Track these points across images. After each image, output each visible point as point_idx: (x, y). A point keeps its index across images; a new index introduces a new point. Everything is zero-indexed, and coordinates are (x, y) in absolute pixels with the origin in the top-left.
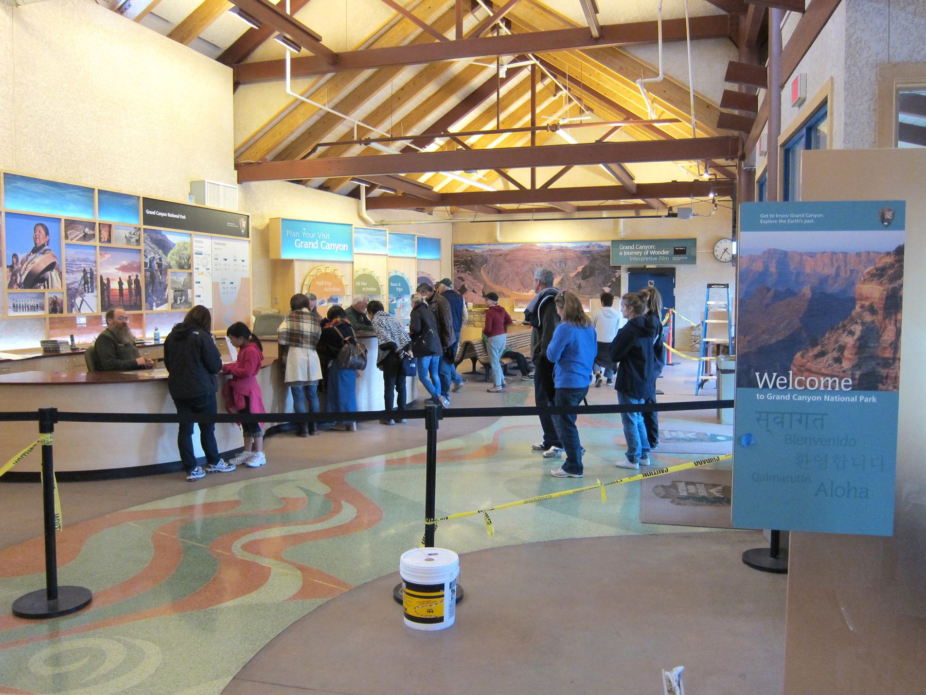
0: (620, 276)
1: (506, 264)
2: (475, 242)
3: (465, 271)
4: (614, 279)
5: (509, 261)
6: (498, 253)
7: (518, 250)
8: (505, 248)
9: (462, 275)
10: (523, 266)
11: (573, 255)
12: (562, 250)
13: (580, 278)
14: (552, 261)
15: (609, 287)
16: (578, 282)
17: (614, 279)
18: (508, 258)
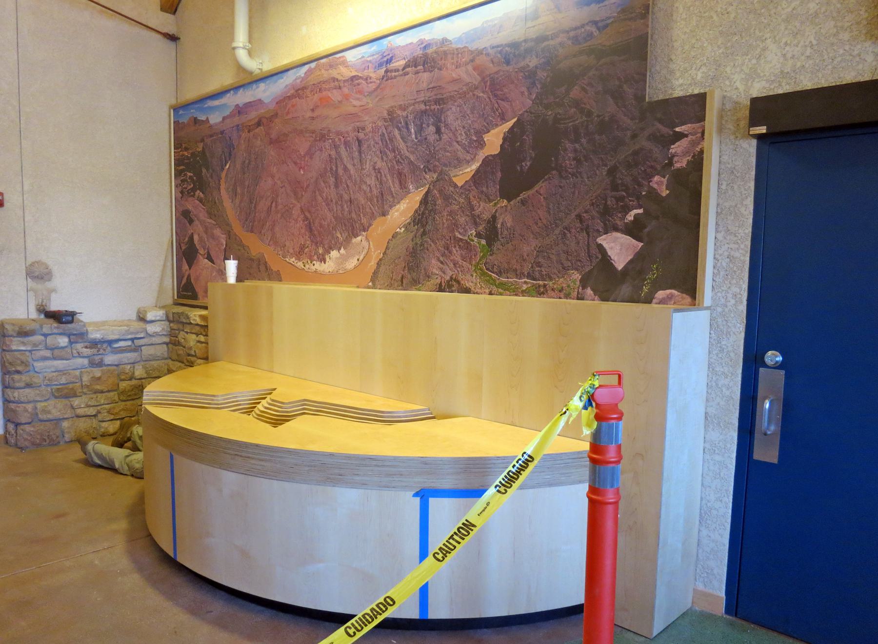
0: (698, 163)
1: (272, 153)
2: (213, 86)
3: (194, 190)
4: (660, 184)
5: (276, 142)
6: (253, 115)
7: (298, 92)
8: (267, 93)
9: (191, 204)
10: (310, 154)
11: (468, 75)
12: (427, 60)
13: (493, 189)
14: (391, 117)
15: (634, 230)
16: (485, 210)
17: (660, 184)
18: (278, 127)
